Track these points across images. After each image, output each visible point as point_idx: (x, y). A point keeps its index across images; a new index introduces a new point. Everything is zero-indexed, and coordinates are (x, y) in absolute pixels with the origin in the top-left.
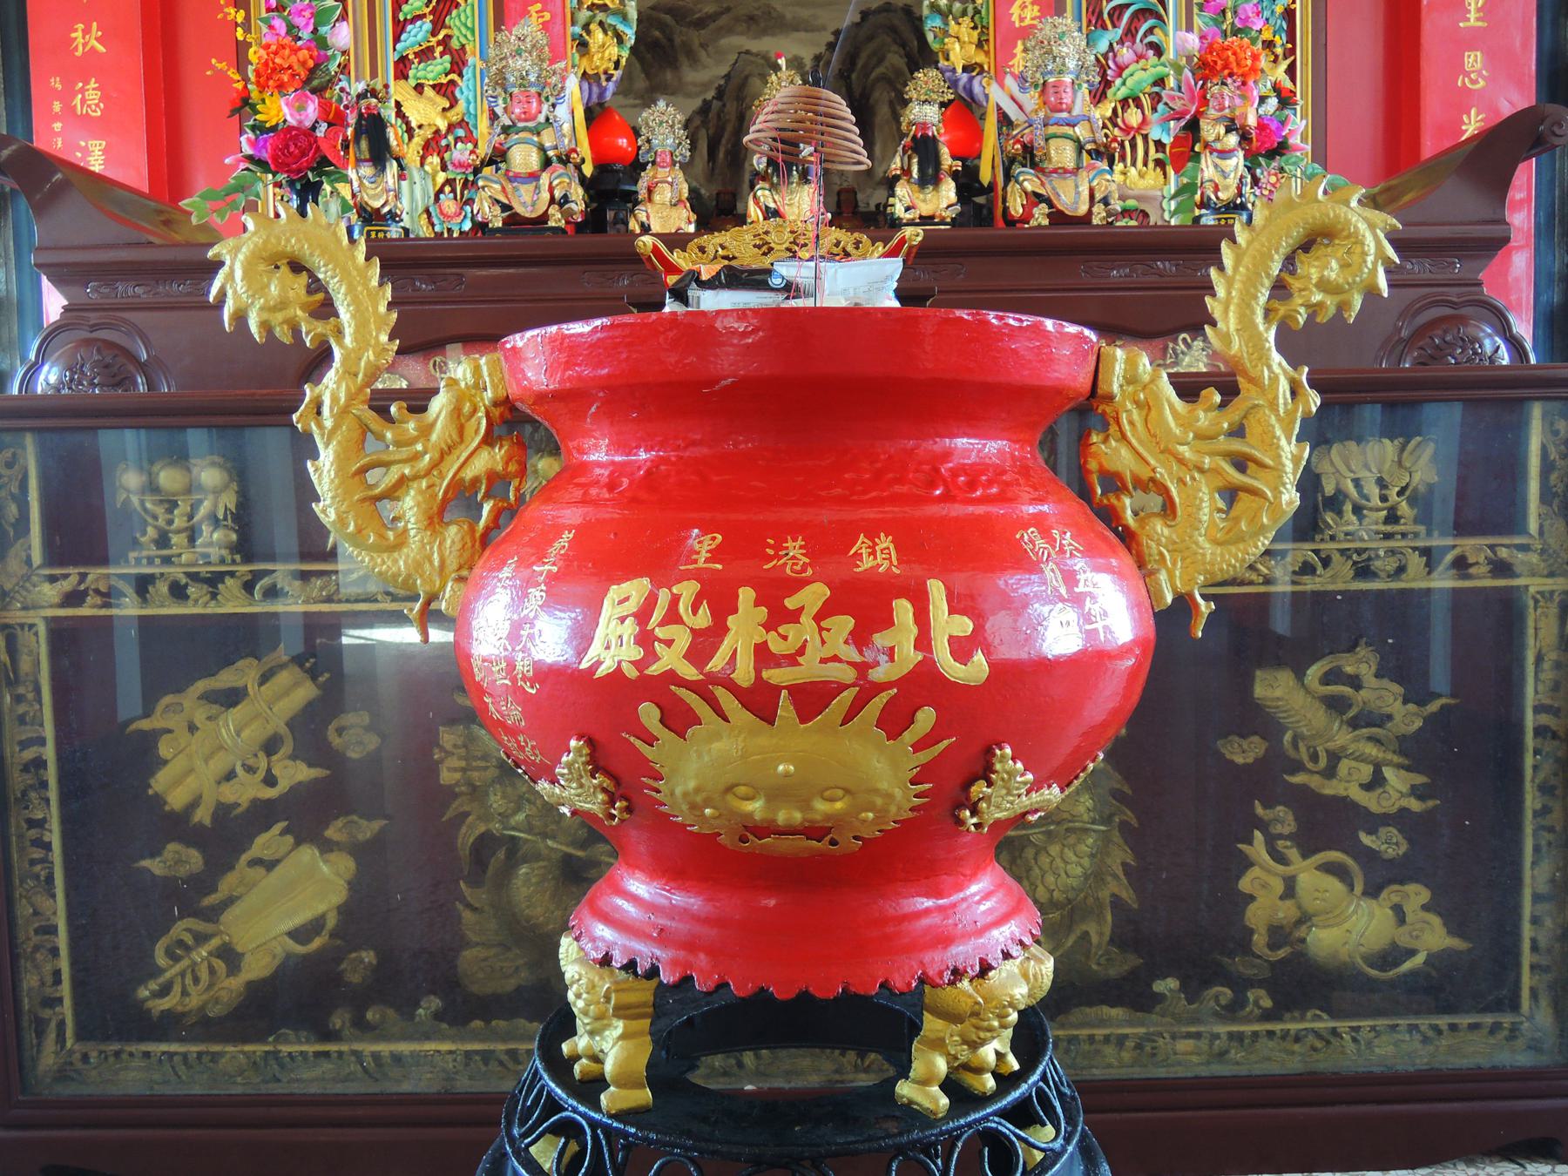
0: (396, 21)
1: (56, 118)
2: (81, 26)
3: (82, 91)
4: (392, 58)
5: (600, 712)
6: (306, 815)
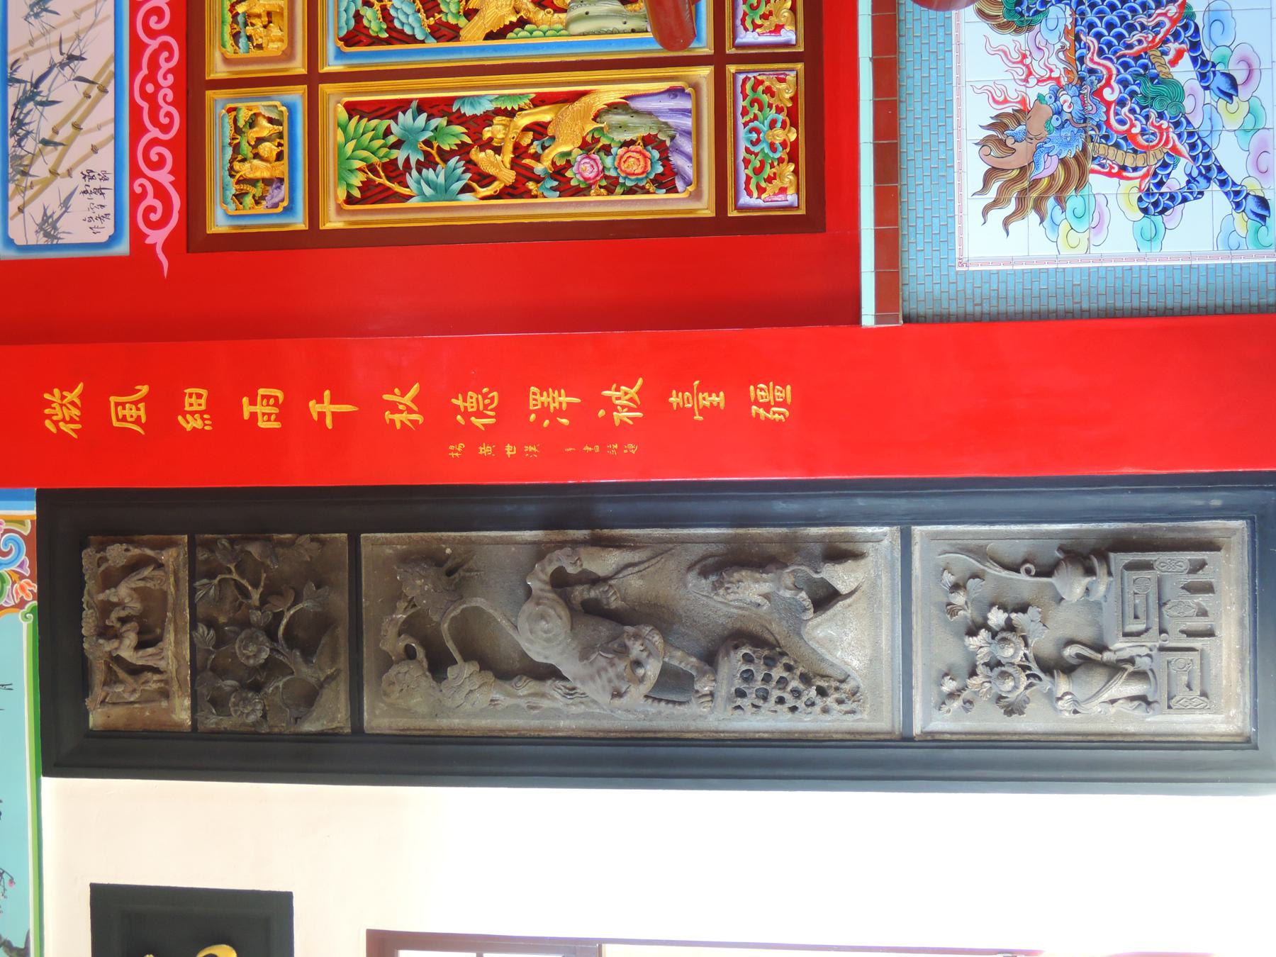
0: (388, 41)
1: (499, 451)
2: (388, 415)
3: (467, 415)
4: (432, 43)
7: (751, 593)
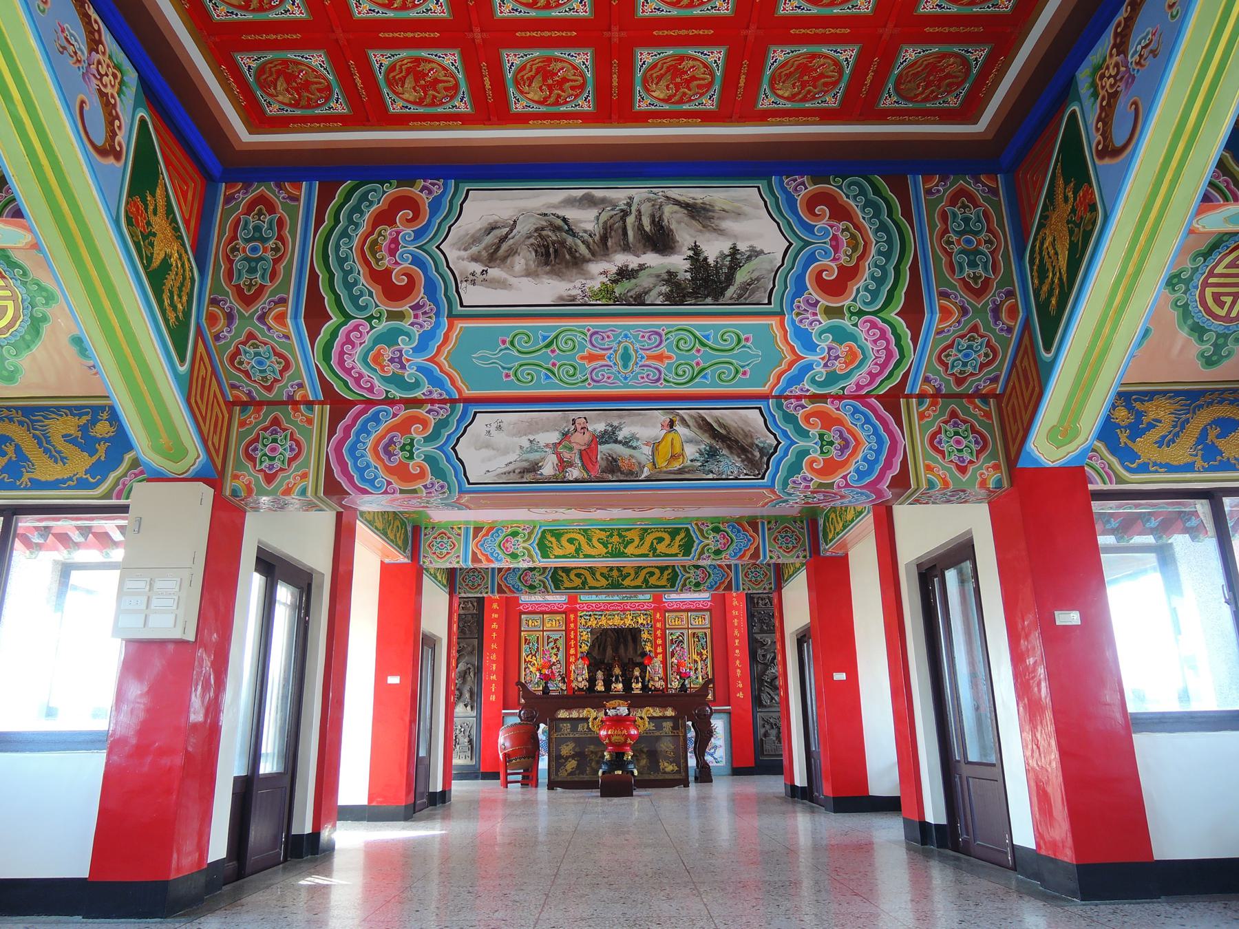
5: (608, 736)
6: (573, 757)
7: (467, 695)
